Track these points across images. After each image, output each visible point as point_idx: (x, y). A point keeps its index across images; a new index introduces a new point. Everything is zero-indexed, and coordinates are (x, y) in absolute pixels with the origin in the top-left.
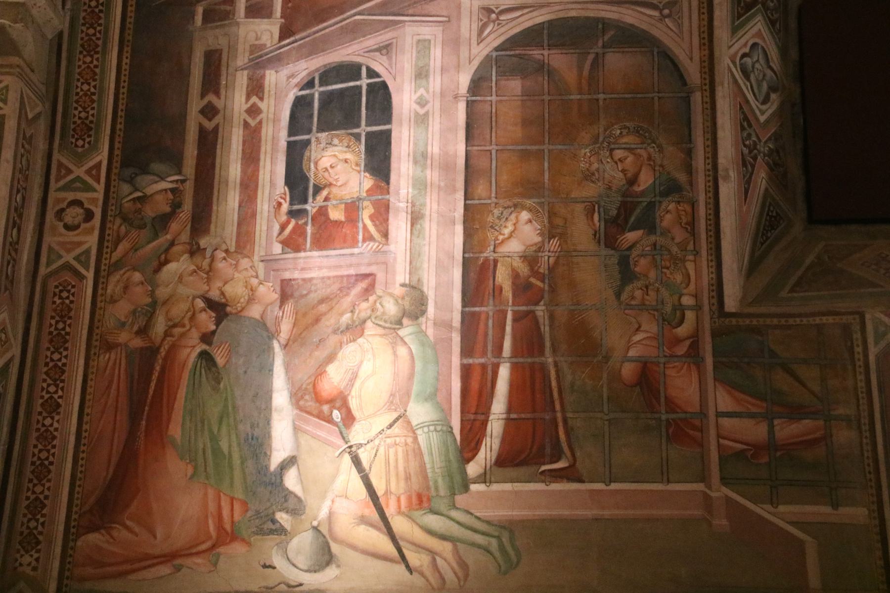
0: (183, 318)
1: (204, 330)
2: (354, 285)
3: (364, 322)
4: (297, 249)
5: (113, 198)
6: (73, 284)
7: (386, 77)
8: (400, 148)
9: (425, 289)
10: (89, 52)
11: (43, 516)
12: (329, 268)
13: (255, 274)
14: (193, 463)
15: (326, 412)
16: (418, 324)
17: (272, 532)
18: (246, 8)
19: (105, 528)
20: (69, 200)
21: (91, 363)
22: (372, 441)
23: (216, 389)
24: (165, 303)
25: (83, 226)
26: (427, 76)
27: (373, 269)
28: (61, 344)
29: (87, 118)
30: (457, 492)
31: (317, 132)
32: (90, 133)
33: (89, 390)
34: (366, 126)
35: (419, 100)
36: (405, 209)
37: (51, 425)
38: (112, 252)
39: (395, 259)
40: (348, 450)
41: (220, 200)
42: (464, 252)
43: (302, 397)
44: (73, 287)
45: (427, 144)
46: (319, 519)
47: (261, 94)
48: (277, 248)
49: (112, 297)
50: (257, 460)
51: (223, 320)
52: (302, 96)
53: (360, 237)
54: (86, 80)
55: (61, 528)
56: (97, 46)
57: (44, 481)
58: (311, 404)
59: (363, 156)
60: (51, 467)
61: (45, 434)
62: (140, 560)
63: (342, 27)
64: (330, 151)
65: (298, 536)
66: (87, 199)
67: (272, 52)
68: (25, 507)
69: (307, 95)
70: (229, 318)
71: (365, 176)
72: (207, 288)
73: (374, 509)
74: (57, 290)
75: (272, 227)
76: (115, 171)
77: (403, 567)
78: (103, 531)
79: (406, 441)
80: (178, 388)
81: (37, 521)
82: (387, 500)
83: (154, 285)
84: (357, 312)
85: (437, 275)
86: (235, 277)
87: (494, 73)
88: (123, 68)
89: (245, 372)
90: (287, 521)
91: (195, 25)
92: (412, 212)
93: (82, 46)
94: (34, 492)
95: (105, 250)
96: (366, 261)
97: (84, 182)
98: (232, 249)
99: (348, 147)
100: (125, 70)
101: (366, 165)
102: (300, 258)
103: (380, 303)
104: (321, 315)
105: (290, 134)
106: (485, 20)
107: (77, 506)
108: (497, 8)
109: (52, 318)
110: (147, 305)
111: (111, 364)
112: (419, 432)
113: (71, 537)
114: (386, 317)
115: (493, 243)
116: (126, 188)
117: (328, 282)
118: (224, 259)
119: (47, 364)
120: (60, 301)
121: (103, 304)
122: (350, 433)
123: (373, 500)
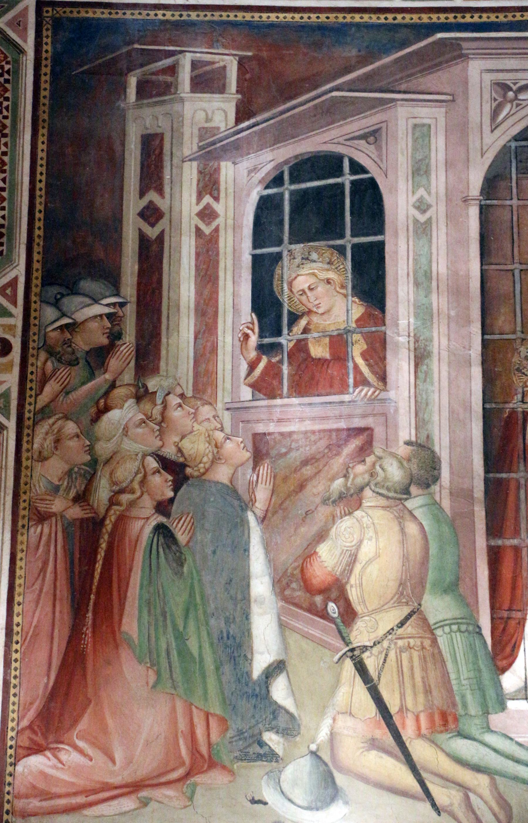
0: (132, 481)
1: (159, 498)
2: (346, 441)
3: (361, 489)
4: (272, 395)
5: (35, 325)
7: (375, 172)
8: (397, 266)
9: (437, 449)
12: (313, 419)
13: (219, 426)
14: (155, 668)
15: (319, 606)
16: (430, 494)
17: (259, 757)
18: (192, 79)
19: (50, 749)
21: (20, 538)
22: (379, 643)
23: (179, 574)
24: (107, 462)
26: (427, 173)
27: (369, 422)
30: (490, 710)
31: (290, 243)
33: (18, 572)
34: (353, 236)
35: (418, 204)
36: (407, 346)
38: (37, 395)
39: (396, 410)
40: (350, 654)
41: (171, 328)
42: (484, 402)
43: (288, 585)
45: (430, 261)
46: (318, 741)
47: (216, 192)
48: (246, 393)
49: (40, 452)
50: (235, 664)
51: (182, 485)
52: (269, 196)
53: (351, 381)
58: (299, 594)
59: (350, 275)
62: (95, 791)
63: (315, 107)
64: (307, 269)
65: (293, 763)
67: (227, 137)
69: (275, 195)
70: (190, 482)
71: (353, 301)
72: (160, 443)
73: (387, 730)
75: (239, 365)
77: (428, 805)
78: (48, 753)
79: (422, 643)
80: (131, 570)
82: (403, 719)
83: (93, 439)
84: (352, 476)
85: (451, 431)
86: (195, 429)
87: (514, 170)
88: (39, 157)
89: (214, 552)
90: (278, 743)
91: (127, 101)
92: (415, 349)
95: (28, 393)
96: (359, 411)
98: (189, 393)
99: (330, 263)
101: (353, 288)
102: (275, 406)
103: (381, 466)
104: (306, 480)
105: (256, 244)
106: (500, 100)
107: (13, 720)
108: (515, 84)
110: (84, 464)
111: (44, 538)
112: (439, 632)
113: (9, 760)
114: (389, 484)
115: (520, 390)
116: (50, 313)
117: (313, 438)
118: (180, 406)
121: (29, 463)
122: (351, 631)
123: (384, 718)
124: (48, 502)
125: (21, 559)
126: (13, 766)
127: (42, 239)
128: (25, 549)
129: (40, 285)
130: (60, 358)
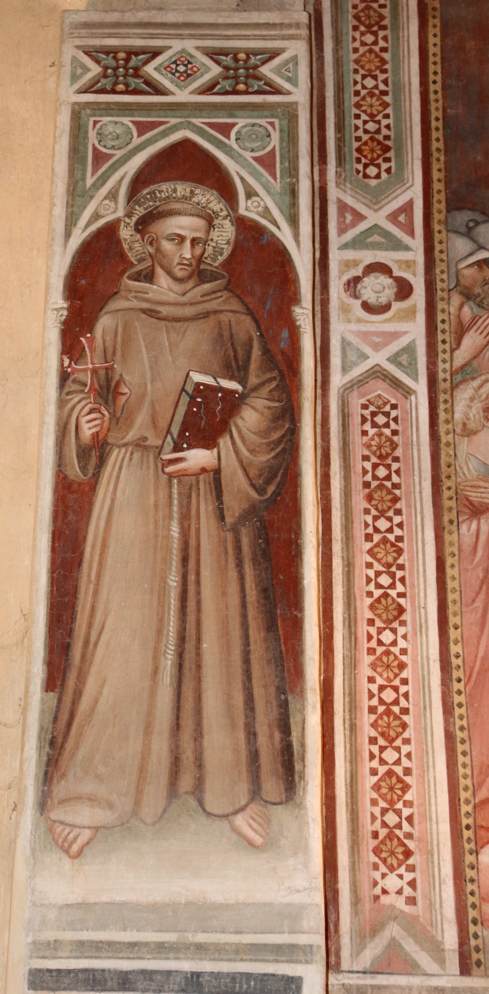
5: (442, 260)
6: (393, 401)
10: (369, 26)
11: (408, 804)
20: (367, 262)
21: (447, 538)
25: (396, 306)
28: (389, 504)
29: (378, 131)
32: (387, 155)
33: (450, 584)
37: (394, 643)
38: (452, 351)
44: (394, 407)
49: (464, 424)
54: (369, 70)
55: (445, 828)
56: (382, 17)
57: (398, 742)
60: (405, 718)
61: (385, 659)
66: (397, 261)
68: (372, 788)
74: (367, 413)
76: (437, 217)
81: (399, 813)
88: (431, 53)
93: (357, 17)
94: (382, 762)
95: (441, 347)
97: (386, 234)
100: (434, 55)
107: (466, 789)
109: (366, 458)
113: (467, 846)
119: (369, 538)
120: (375, 430)
124: (482, 490)
125: (453, 566)
126: (475, 854)
127: (443, 152)
128: (456, 552)
129: (444, 211)
130: (481, 301)
